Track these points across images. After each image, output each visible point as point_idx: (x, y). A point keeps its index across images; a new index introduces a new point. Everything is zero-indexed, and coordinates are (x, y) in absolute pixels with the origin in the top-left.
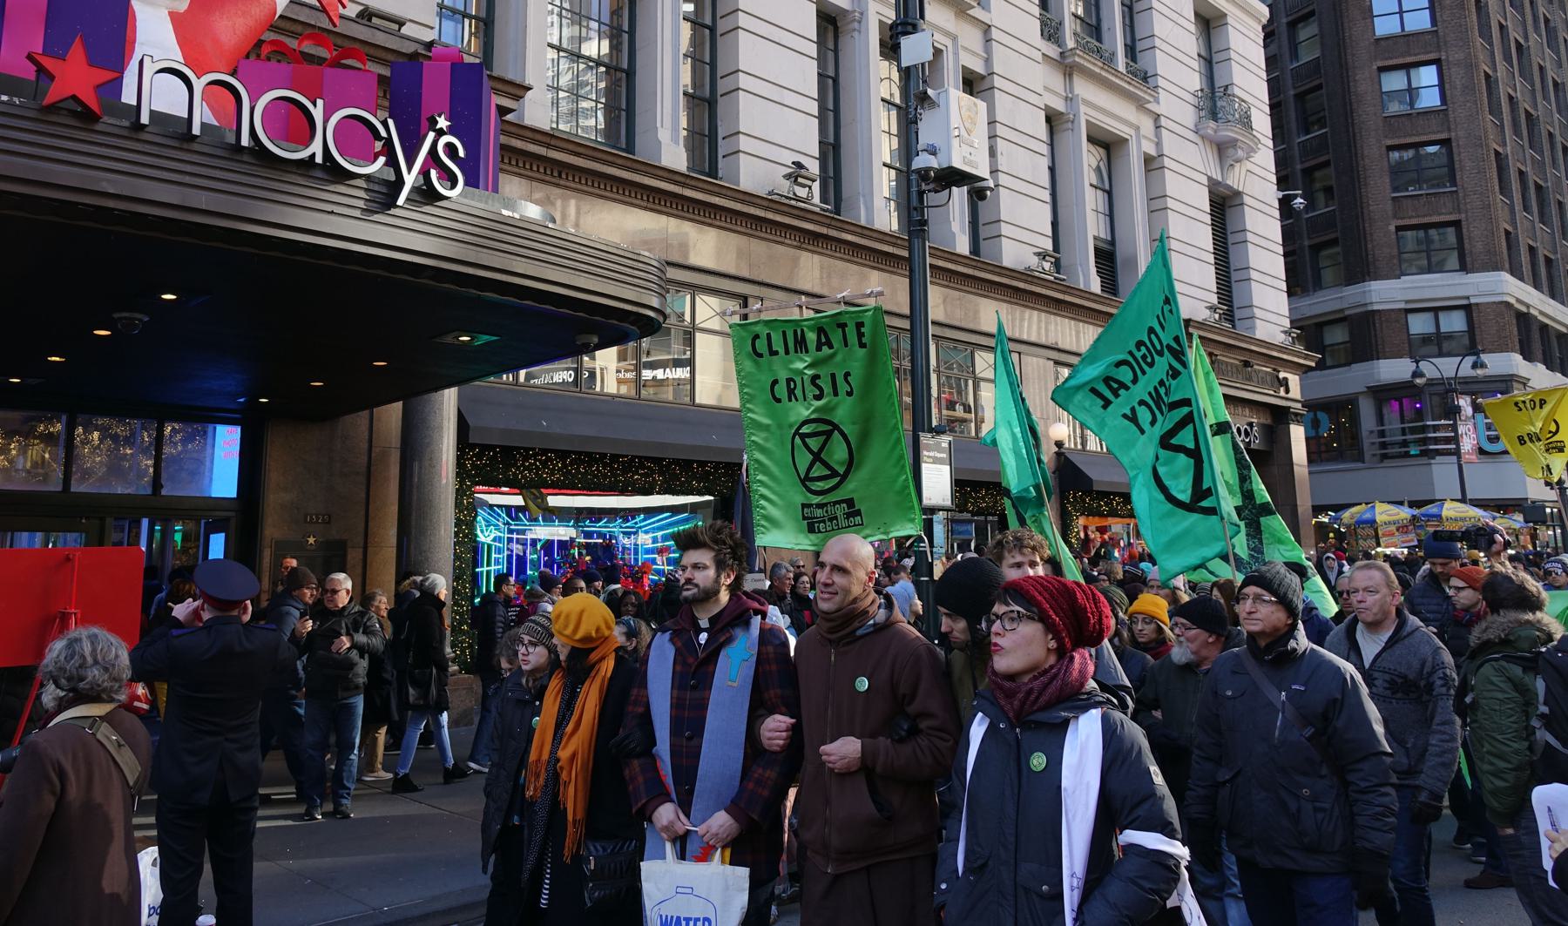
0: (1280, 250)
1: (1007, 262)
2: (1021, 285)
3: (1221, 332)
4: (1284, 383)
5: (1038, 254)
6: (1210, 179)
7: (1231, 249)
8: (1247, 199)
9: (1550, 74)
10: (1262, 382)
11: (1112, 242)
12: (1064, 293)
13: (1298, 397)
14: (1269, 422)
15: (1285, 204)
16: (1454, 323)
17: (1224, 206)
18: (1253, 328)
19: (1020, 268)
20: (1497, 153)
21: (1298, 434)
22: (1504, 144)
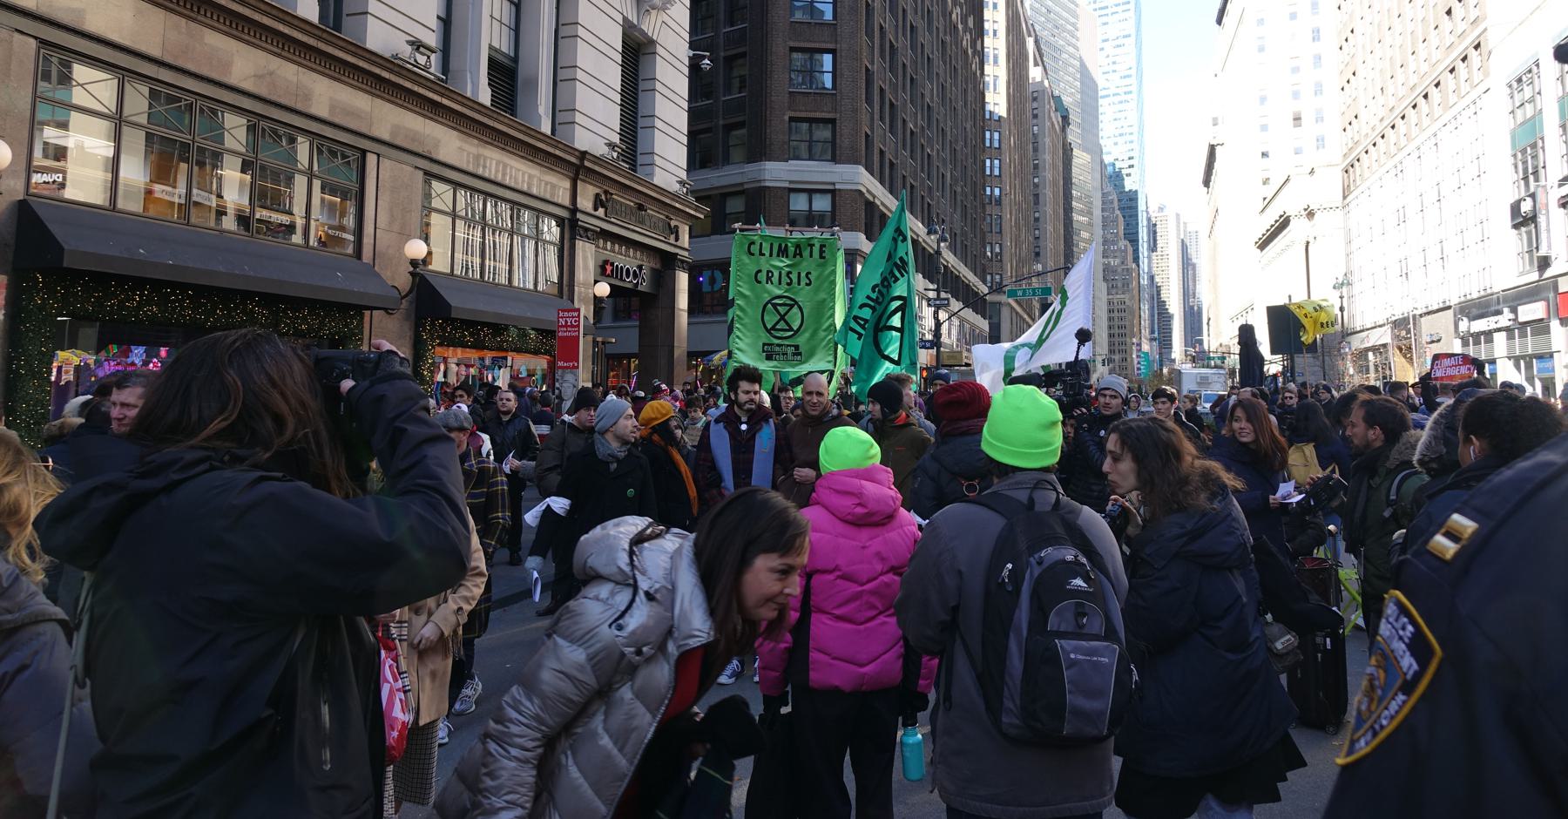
0: (685, 105)
1: (372, 43)
2: (385, 75)
3: (617, 170)
4: (675, 231)
5: (411, 43)
6: (625, 19)
7: (641, 94)
8: (659, 50)
9: (909, 17)
10: (654, 227)
11: (515, 60)
12: (442, 95)
13: (686, 245)
14: (658, 266)
15: (694, 66)
16: (822, 204)
17: (636, 52)
18: (652, 174)
19: (387, 55)
20: (867, 69)
21: (683, 279)
22: (872, 63)
